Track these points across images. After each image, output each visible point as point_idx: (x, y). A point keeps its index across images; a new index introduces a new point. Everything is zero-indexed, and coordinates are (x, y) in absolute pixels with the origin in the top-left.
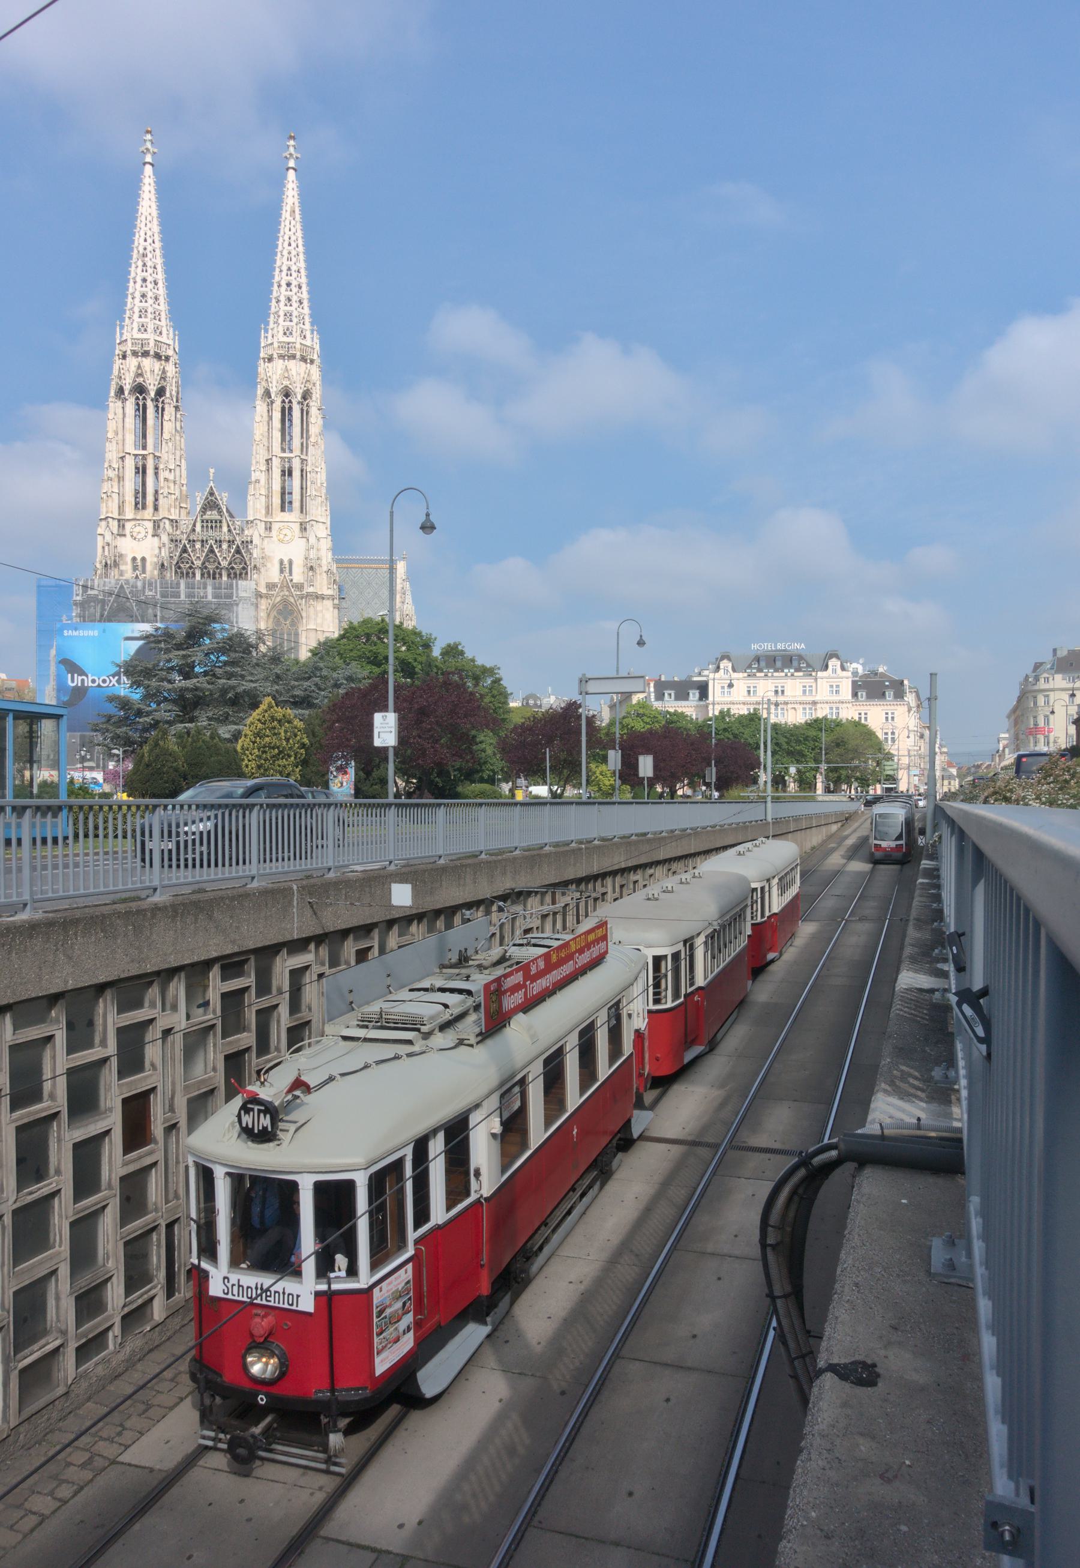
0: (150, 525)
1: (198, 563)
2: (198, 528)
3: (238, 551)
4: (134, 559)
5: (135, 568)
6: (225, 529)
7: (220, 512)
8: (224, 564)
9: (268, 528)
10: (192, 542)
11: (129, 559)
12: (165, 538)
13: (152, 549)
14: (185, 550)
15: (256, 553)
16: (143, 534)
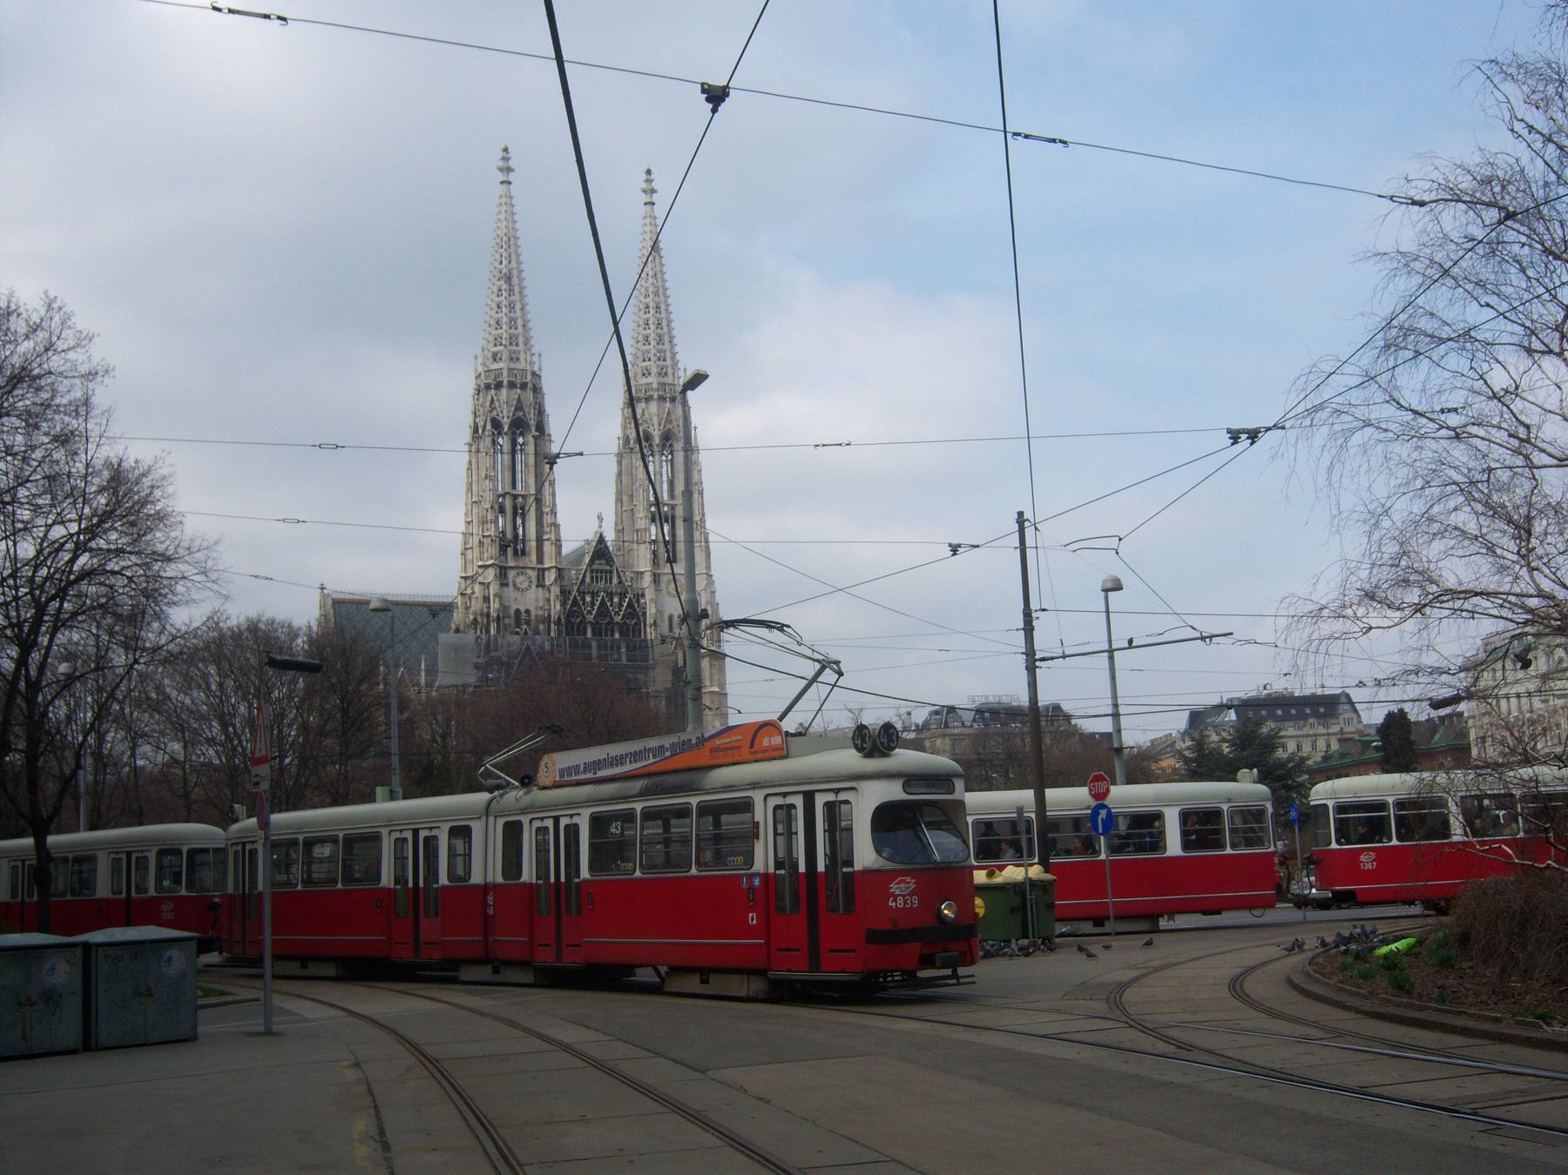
0: (533, 574)
1: (590, 618)
2: (588, 580)
3: (630, 605)
4: (518, 612)
5: (518, 624)
6: (615, 581)
7: (610, 561)
8: (618, 619)
9: (656, 579)
10: (582, 594)
11: (512, 612)
12: (555, 590)
13: (537, 600)
14: (575, 602)
15: (651, 610)
16: (526, 584)
